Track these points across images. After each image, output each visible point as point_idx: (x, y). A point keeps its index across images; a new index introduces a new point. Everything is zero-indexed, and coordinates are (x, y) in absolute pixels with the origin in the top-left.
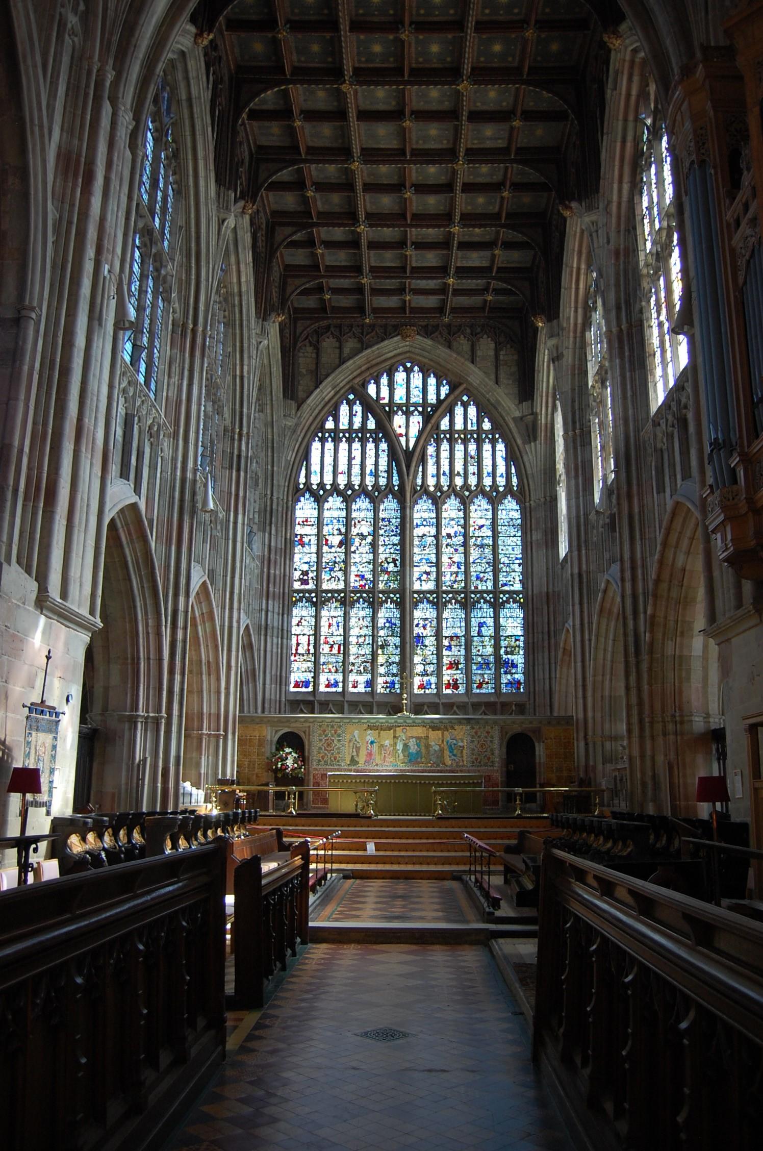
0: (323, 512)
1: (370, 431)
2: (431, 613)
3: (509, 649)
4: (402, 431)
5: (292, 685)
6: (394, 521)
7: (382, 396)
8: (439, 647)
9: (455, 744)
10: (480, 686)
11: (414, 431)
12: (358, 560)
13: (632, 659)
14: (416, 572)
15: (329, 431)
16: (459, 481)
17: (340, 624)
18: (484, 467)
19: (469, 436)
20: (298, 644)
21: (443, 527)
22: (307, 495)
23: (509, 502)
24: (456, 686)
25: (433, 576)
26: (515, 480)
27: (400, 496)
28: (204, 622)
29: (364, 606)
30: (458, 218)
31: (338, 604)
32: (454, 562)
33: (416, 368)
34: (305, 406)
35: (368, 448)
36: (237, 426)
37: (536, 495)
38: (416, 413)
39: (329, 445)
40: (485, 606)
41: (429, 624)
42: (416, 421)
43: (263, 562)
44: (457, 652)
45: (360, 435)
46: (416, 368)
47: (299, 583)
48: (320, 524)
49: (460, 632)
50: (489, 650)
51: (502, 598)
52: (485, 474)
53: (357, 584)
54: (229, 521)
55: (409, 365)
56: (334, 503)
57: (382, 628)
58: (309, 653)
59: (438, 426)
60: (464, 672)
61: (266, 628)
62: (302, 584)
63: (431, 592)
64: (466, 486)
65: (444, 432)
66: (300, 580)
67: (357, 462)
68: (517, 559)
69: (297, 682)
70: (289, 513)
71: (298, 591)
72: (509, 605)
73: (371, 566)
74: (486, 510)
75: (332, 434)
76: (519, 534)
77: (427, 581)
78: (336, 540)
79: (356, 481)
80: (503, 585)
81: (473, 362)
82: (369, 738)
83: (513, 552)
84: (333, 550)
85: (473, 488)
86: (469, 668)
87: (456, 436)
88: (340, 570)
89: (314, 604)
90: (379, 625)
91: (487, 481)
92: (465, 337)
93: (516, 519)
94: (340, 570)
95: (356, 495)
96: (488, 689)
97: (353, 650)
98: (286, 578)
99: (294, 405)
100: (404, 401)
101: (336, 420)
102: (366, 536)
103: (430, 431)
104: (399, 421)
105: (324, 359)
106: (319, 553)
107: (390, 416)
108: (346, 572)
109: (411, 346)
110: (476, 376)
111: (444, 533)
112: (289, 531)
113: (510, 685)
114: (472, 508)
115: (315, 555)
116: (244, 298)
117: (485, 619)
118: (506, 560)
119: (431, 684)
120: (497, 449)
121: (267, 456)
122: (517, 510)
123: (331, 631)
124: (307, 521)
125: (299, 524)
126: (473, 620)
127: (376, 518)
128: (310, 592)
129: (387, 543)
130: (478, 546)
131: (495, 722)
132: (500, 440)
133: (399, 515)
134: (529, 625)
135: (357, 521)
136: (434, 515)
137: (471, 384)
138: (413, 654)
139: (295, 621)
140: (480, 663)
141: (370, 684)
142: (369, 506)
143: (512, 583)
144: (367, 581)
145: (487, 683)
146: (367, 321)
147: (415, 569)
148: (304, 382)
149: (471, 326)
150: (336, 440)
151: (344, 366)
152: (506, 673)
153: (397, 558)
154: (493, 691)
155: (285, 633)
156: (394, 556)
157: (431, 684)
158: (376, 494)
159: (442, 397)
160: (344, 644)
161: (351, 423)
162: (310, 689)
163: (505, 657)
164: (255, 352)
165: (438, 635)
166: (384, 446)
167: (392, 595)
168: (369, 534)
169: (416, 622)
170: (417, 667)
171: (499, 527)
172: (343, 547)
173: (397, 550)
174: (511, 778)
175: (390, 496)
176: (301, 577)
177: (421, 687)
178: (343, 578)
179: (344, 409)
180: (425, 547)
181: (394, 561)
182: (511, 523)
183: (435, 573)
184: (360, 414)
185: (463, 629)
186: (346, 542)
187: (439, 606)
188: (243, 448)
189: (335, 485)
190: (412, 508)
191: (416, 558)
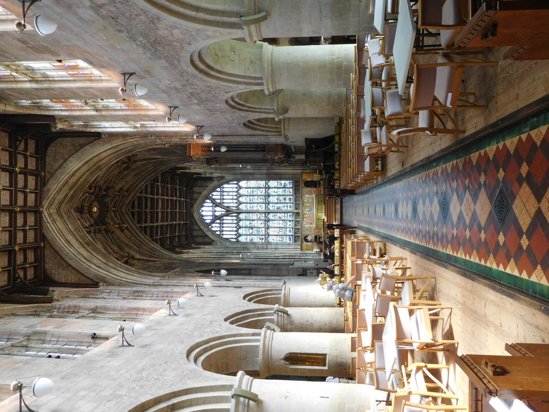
2: (271, 205)
10: (290, 192)
11: (221, 209)
14: (260, 209)
15: (220, 233)
16: (235, 197)
24: (290, 199)
25: (261, 204)
26: (235, 182)
27: (239, 213)
34: (214, 240)
39: (224, 233)
42: (218, 209)
44: (282, 198)
46: (202, 209)
49: (276, 197)
50: (281, 189)
55: (201, 211)
56: (240, 231)
64: (236, 195)
67: (230, 225)
78: (251, 230)
82: (306, 220)
89: (269, 236)
95: (238, 225)
96: (291, 190)
97: (281, 226)
98: (262, 244)
99: (214, 243)
101: (217, 231)
104: (217, 214)
105: (200, 234)
106: (255, 235)
107: (216, 216)
108: (260, 228)
110: (205, 193)
114: (242, 194)
134: (274, 179)
139: (273, 241)
141: (290, 221)
148: (207, 240)
155: (277, 244)
161: (218, 227)
162: (291, 237)
163: (283, 186)
165: (277, 203)
166: (224, 218)
174: (316, 187)
177: (291, 208)
179: (214, 229)
186: (252, 228)
189: (236, 231)
191: (256, 209)
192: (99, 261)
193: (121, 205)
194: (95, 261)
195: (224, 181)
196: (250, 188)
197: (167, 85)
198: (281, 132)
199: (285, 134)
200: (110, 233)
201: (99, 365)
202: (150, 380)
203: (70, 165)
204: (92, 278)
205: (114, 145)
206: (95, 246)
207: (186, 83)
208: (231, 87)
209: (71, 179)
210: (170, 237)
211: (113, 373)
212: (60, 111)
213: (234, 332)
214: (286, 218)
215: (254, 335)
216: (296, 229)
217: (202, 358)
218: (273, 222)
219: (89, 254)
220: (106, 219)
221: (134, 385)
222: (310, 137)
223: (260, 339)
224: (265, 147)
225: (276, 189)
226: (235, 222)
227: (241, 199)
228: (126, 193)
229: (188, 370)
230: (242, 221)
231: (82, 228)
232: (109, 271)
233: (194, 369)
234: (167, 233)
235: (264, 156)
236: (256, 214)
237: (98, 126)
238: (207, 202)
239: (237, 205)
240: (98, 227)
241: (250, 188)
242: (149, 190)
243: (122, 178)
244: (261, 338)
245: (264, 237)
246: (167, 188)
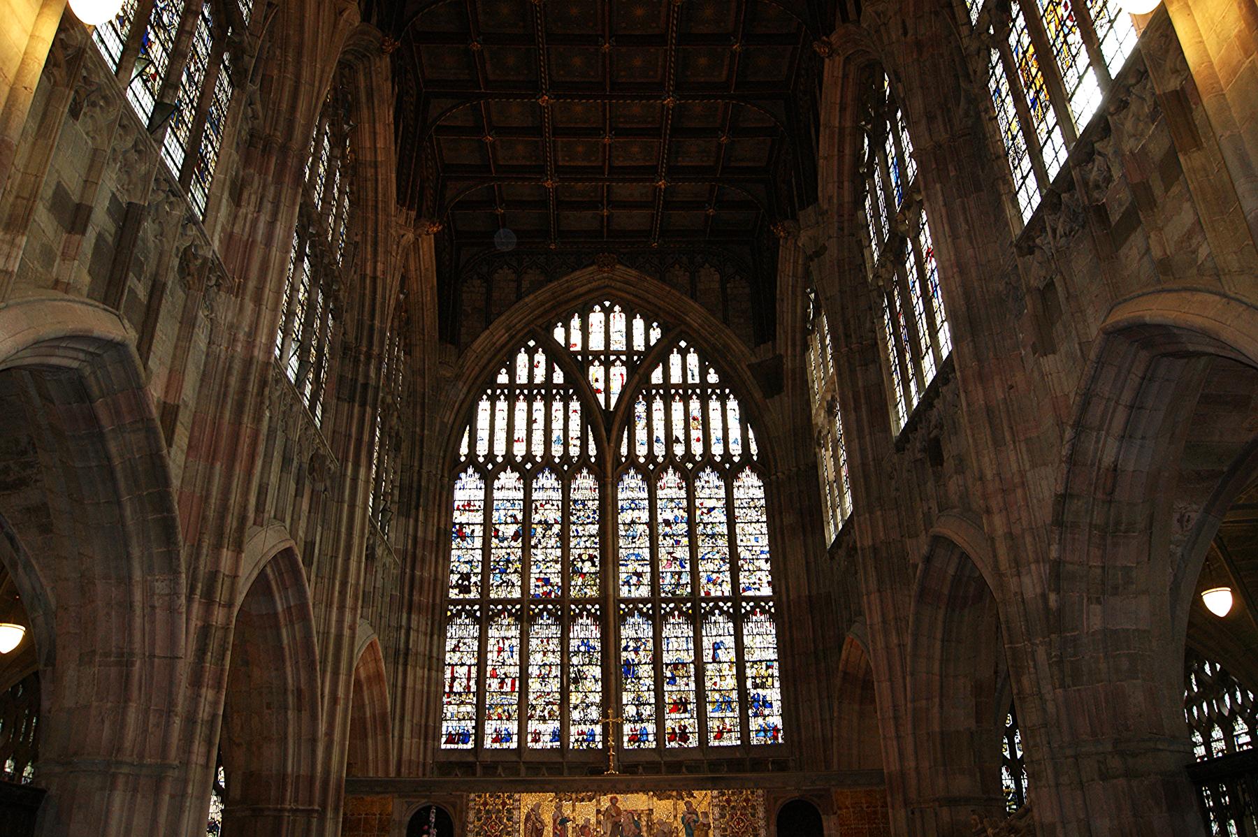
0: (492, 493)
1: (558, 386)
2: (647, 631)
3: (758, 681)
5: (444, 739)
6: (590, 503)
7: (572, 341)
8: (659, 680)
9: (695, 822)
10: (719, 736)
11: (616, 387)
12: (540, 558)
15: (502, 386)
16: (679, 450)
17: (515, 649)
18: (712, 431)
19: (690, 391)
20: (453, 679)
21: (659, 511)
22: (470, 471)
23: (747, 476)
24: (684, 736)
25: (646, 579)
26: (754, 448)
27: (598, 471)
28: (291, 621)
29: (550, 622)
31: (511, 620)
32: (675, 559)
33: (617, 308)
35: (554, 408)
36: (365, 342)
38: (618, 363)
39: (502, 405)
40: (721, 619)
41: (643, 647)
42: (619, 373)
43: (405, 559)
45: (543, 391)
46: (617, 308)
47: (456, 591)
49: (688, 657)
50: (731, 683)
51: (745, 608)
52: (713, 440)
53: (540, 591)
54: (345, 475)
55: (607, 304)
56: (508, 479)
57: (576, 653)
58: (469, 692)
59: (649, 378)
60: (695, 716)
61: (406, 654)
62: (460, 592)
63: (644, 601)
65: (657, 387)
66: (457, 586)
67: (539, 426)
68: (762, 552)
69: (450, 734)
70: (445, 493)
71: (455, 602)
72: (754, 618)
73: (559, 566)
74: (717, 487)
75: (506, 391)
76: (764, 518)
78: (511, 530)
79: (538, 450)
80: (744, 590)
81: (692, 298)
83: (756, 544)
84: (506, 544)
85: (698, 459)
86: (703, 709)
87: (673, 391)
88: (516, 571)
89: (477, 621)
90: (571, 649)
91: (717, 450)
92: (681, 267)
93: (759, 499)
94: (514, 572)
95: (538, 469)
96: (732, 740)
97: (534, 685)
100: (602, 348)
101: (512, 373)
102: (552, 525)
103: (638, 385)
104: (596, 372)
106: (486, 549)
108: (524, 574)
109: (611, 279)
110: (695, 315)
111: (660, 520)
112: (443, 519)
113: (762, 734)
115: (480, 552)
116: (381, 171)
117: (722, 638)
119: (647, 734)
120: (728, 407)
121: (414, 414)
122: (760, 487)
124: (469, 505)
125: (458, 509)
126: (705, 639)
127: (566, 500)
128: (472, 602)
129: (580, 534)
130: (708, 536)
132: (732, 396)
133: (596, 495)
135: (538, 504)
136: (645, 495)
137: (689, 326)
138: (620, 689)
139: (450, 645)
140: (717, 701)
141: (560, 735)
142: (556, 484)
143: (757, 586)
144: (553, 587)
145: (730, 731)
146: (553, 247)
147: (622, 569)
150: (512, 400)
151: (521, 303)
152: (756, 715)
153: (596, 553)
154: (739, 742)
155: (436, 662)
156: (591, 551)
157: (647, 734)
158: (566, 467)
159: (653, 342)
160: (520, 678)
161: (531, 376)
162: (470, 745)
163: (753, 692)
164: (395, 247)
165: (657, 662)
166: (575, 405)
167: (589, 607)
168: (556, 522)
169: (624, 643)
170: (627, 709)
171: (736, 510)
172: (520, 540)
173: (596, 543)
175: (585, 472)
176: (460, 582)
177: (633, 739)
178: (519, 583)
179: (522, 359)
180: (634, 537)
181: (591, 558)
182: (752, 504)
183: (648, 575)
184: (543, 365)
185: (692, 653)
186: (525, 533)
187: (657, 620)
188: (372, 374)
189: (509, 456)
195: (758, 395)
196: (731, 521)
218: (554, 645)
227: (671, 478)
236: (596, 553)
241: (731, 521)
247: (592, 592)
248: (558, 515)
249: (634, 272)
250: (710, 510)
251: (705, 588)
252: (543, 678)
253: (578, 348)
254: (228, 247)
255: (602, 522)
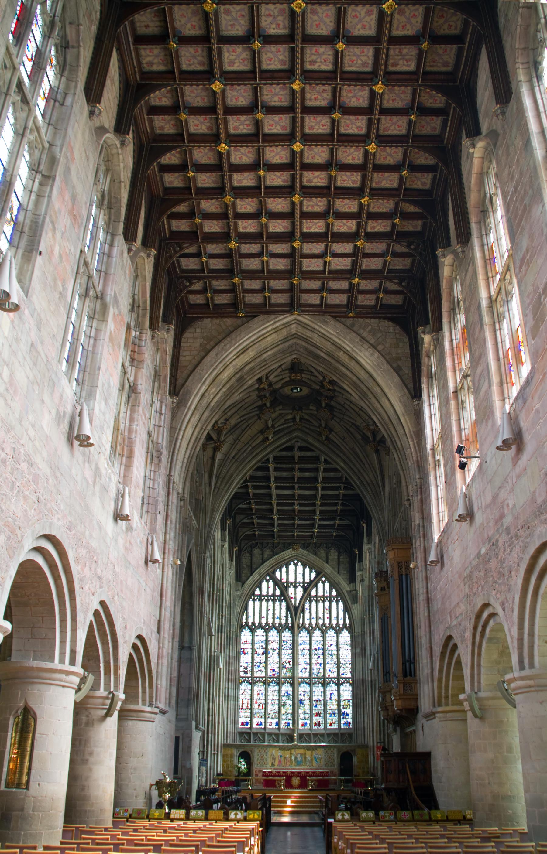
1: (277, 596)
2: (307, 689)
4: (293, 596)
8: (311, 706)
10: (331, 725)
13: (382, 728)
14: (300, 668)
15: (258, 596)
16: (321, 622)
22: (247, 628)
24: (319, 725)
25: (308, 670)
26: (348, 622)
27: (292, 629)
30: (318, 513)
33: (300, 564)
34: (246, 585)
37: (358, 630)
39: (257, 603)
42: (300, 591)
44: (320, 708)
46: (300, 564)
48: (253, 643)
49: (322, 698)
50: (335, 707)
52: (333, 618)
53: (271, 674)
55: (296, 561)
56: (260, 632)
63: (307, 678)
64: (324, 624)
65: (314, 596)
67: (271, 612)
71: (243, 677)
73: (278, 665)
77: (306, 672)
78: (260, 651)
82: (280, 754)
89: (251, 684)
91: (334, 622)
96: (335, 726)
97: (270, 707)
98: (237, 671)
99: (240, 584)
101: (261, 590)
104: (291, 590)
105: (255, 560)
106: (253, 658)
107: (287, 588)
108: (266, 667)
110: (328, 569)
111: (313, 648)
114: (327, 635)
118: (343, 662)
123: (259, 698)
127: (280, 641)
128: (248, 678)
131: (335, 747)
133: (291, 639)
136: (308, 639)
139: (241, 692)
141: (278, 724)
148: (245, 572)
149: (326, 544)
150: (261, 600)
155: (236, 698)
161: (268, 592)
162: (249, 726)
163: (343, 710)
165: (310, 699)
166: (284, 603)
177: (302, 725)
179: (264, 584)
181: (289, 662)
189: (260, 623)
190: (298, 636)
192: (212, 396)
193: (304, 429)
194: (213, 390)
195: (350, 603)
197: (506, 503)
198: (440, 705)
199: (438, 712)
200: (258, 412)
201: (46, 398)
202: (12, 474)
203: (367, 354)
204: (185, 386)
205: (402, 419)
206: (236, 391)
207: (513, 532)
208: (513, 611)
209: (345, 355)
210: (251, 509)
211: (30, 418)
212: (450, 340)
213: (80, 617)
214: (284, 717)
215: (73, 652)
216: (263, 735)
217: (40, 560)
218: (276, 693)
219: (224, 381)
220: (281, 407)
221: (8, 450)
222: (432, 762)
223: (64, 663)
224: (411, 675)
225: (336, 698)
226: (277, 622)
227: (317, 633)
228: (324, 438)
229: (22, 536)
230: (277, 634)
231: (267, 371)
232: (196, 412)
233: (23, 546)
234: (257, 503)
235: (395, 675)
236: (291, 660)
237: (431, 395)
238: (311, 572)
239: (307, 626)
240: (267, 395)
242: (332, 474)
243: (349, 431)
244: (67, 667)
245: (249, 674)
246: (336, 505)
247: (289, 675)
248: (278, 646)
249: (306, 552)
250: (331, 645)
251: (328, 674)
252: (273, 704)
253: (285, 580)
254: (164, 553)
255: (293, 649)
